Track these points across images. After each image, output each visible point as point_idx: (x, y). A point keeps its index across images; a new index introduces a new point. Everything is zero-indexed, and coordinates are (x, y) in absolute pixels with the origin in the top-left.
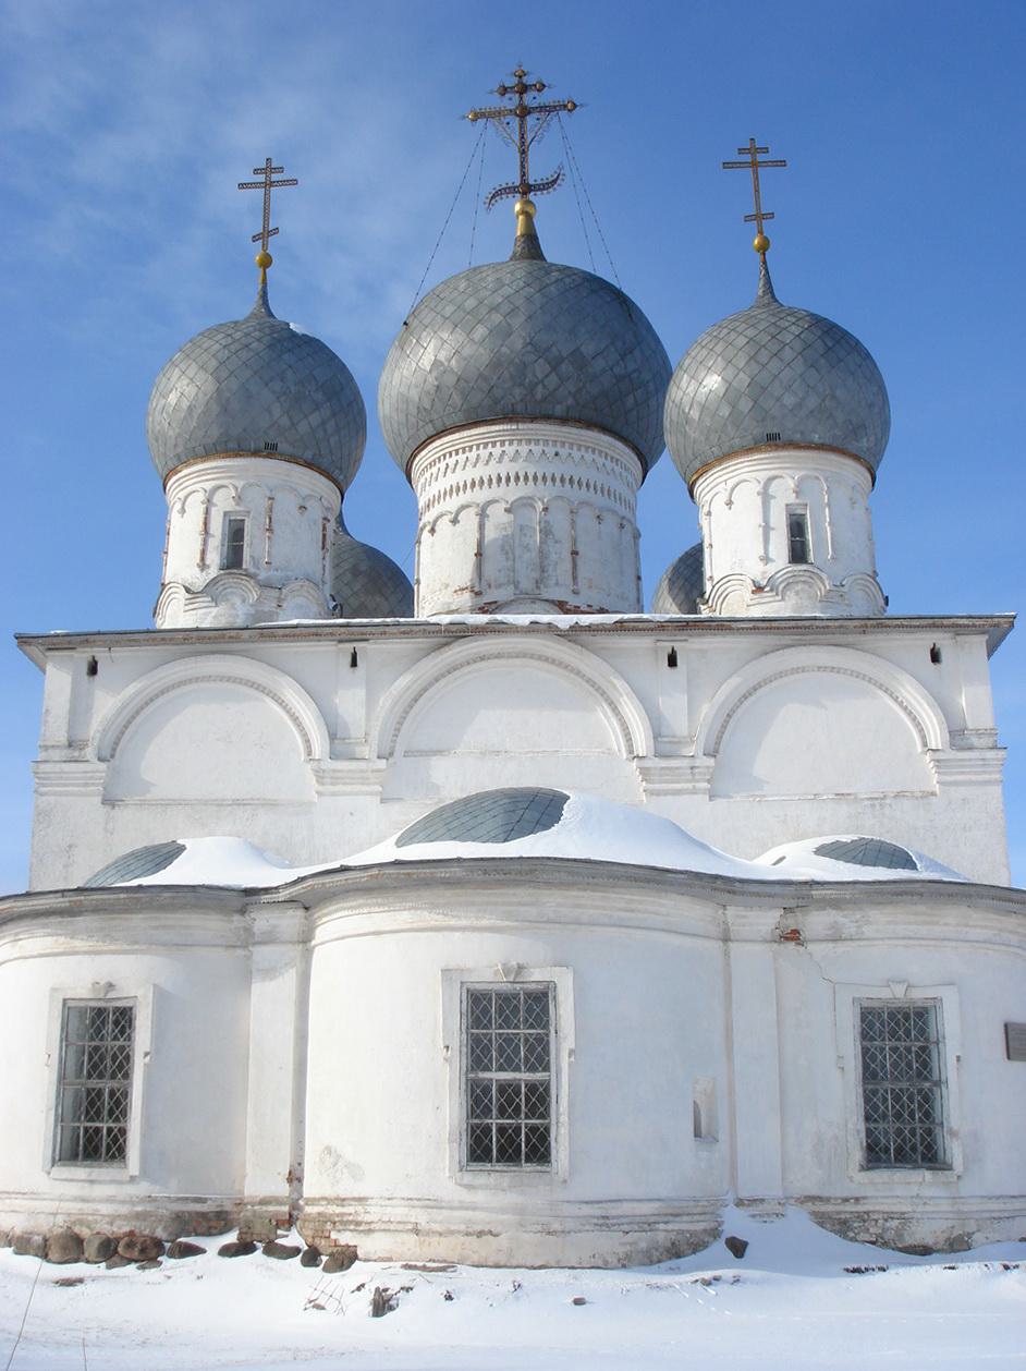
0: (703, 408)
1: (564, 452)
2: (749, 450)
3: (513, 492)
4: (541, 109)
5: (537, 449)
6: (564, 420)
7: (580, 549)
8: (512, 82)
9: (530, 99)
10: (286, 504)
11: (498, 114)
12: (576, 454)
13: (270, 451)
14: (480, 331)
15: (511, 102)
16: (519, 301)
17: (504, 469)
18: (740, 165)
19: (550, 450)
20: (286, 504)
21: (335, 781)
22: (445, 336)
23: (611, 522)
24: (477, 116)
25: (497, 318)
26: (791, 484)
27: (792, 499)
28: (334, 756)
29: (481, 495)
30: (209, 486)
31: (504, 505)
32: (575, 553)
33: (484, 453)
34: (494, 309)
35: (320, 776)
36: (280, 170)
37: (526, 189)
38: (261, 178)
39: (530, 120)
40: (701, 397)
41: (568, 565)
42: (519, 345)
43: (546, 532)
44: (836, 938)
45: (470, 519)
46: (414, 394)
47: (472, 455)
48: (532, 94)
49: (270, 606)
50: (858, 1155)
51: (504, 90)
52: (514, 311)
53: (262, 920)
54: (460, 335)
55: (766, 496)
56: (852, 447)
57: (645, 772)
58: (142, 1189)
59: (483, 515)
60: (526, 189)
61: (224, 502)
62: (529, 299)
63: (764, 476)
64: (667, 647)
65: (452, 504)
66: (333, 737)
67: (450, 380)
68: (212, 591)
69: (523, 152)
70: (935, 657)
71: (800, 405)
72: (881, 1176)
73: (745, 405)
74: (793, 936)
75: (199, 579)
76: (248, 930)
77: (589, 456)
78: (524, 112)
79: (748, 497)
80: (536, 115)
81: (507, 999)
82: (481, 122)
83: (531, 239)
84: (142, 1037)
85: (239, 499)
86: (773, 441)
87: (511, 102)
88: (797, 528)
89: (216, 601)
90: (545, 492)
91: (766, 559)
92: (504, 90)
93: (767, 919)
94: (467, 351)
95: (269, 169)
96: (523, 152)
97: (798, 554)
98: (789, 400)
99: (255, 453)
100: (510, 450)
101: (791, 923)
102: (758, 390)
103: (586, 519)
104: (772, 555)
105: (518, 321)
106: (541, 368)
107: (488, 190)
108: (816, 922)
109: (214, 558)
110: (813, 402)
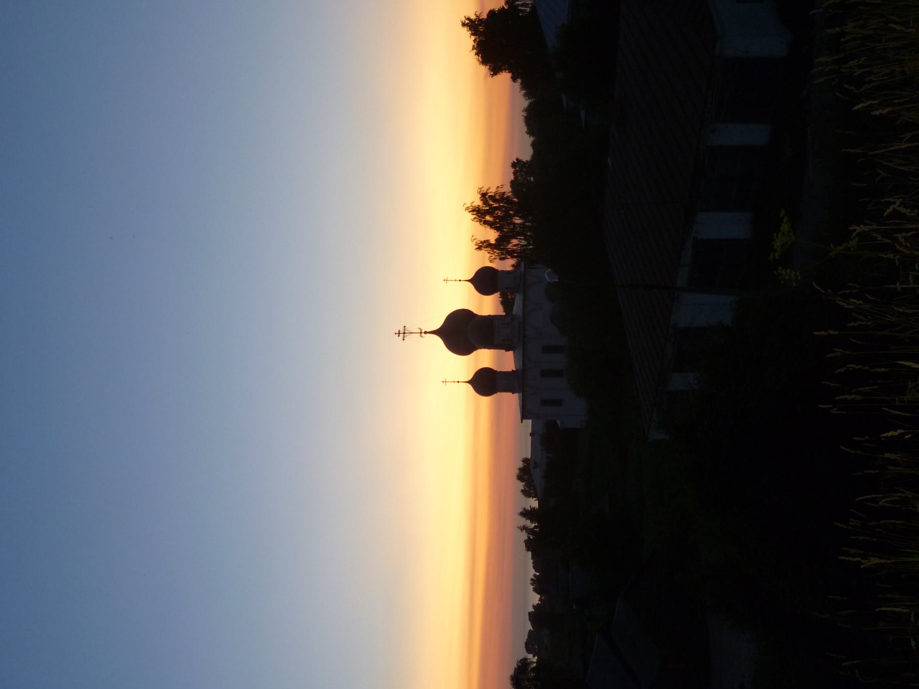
8: (397, 335)
11: (404, 337)
15: (402, 335)
24: (404, 340)
37: (421, 333)
39: (406, 332)
48: (401, 332)
69: (413, 333)
87: (402, 335)
92: (399, 336)
96: (413, 333)
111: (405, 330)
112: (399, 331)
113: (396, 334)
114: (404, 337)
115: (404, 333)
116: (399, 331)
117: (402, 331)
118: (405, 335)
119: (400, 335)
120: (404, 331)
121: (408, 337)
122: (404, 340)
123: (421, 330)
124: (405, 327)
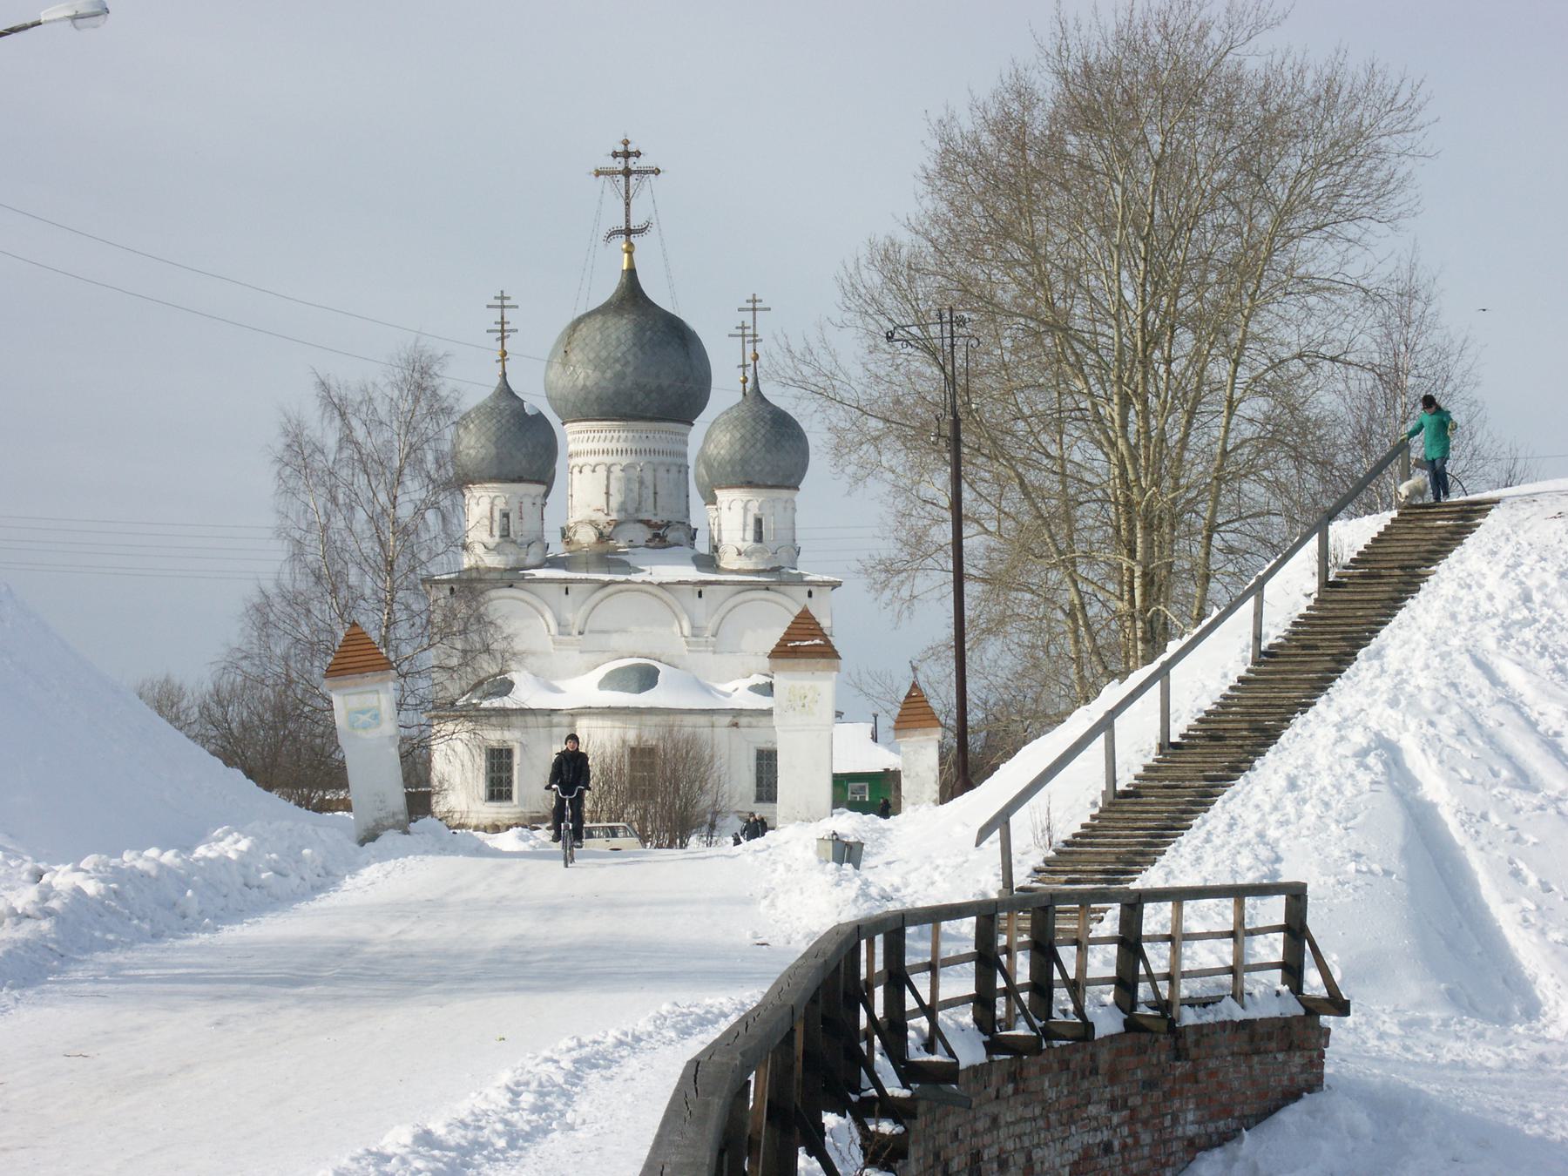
0: (720, 463)
1: (650, 436)
2: (741, 487)
3: (625, 460)
4: (639, 172)
5: (637, 435)
6: (652, 419)
7: (658, 489)
8: (620, 148)
9: (633, 163)
10: (527, 503)
11: (611, 173)
12: (657, 436)
13: (520, 480)
14: (609, 374)
15: (619, 164)
16: (630, 358)
17: (620, 446)
18: (748, 310)
19: (644, 435)
20: (527, 503)
21: (560, 643)
22: (590, 372)
23: (674, 470)
24: (598, 173)
25: (618, 367)
26: (757, 504)
27: (756, 511)
28: (561, 634)
29: (608, 459)
30: (492, 495)
31: (619, 467)
32: (655, 493)
33: (609, 435)
34: (617, 360)
35: (554, 642)
36: (508, 298)
37: (628, 232)
38: (498, 302)
39: (632, 179)
40: (720, 457)
41: (652, 500)
42: (629, 384)
43: (641, 483)
44: (749, 726)
45: (602, 471)
46: (572, 398)
47: (603, 435)
48: (632, 160)
49: (523, 556)
50: (753, 798)
51: (615, 155)
52: (627, 364)
53: (556, 719)
54: (598, 374)
55: (746, 509)
56: (787, 484)
57: (687, 642)
58: (518, 810)
59: (609, 471)
60: (628, 232)
61: (500, 504)
62: (635, 355)
63: (745, 499)
64: (698, 589)
65: (593, 460)
66: (559, 625)
67: (592, 397)
68: (497, 549)
69: (628, 204)
70: (810, 594)
71: (761, 471)
72: (760, 805)
73: (738, 468)
74: (736, 725)
75: (492, 542)
76: (551, 722)
77: (663, 436)
78: (627, 173)
79: (738, 507)
80: (635, 176)
81: (642, 750)
82: (602, 177)
83: (631, 273)
84: (516, 759)
85: (506, 503)
86: (750, 484)
87: (619, 164)
88: (759, 522)
89: (499, 554)
90: (642, 461)
91: (744, 540)
92: (615, 155)
93: (727, 720)
94: (603, 384)
95: (502, 298)
96: (628, 204)
97: (759, 537)
98: (758, 468)
99: (513, 481)
100: (623, 435)
101: (735, 720)
102: (744, 461)
103: (662, 473)
104: (747, 538)
105: (630, 370)
106: (640, 396)
107: (604, 232)
108: (743, 721)
109: (497, 532)
110: (768, 468)
111: (642, 172)
112: (638, 154)
113: (626, 143)
114: (611, 173)
115: (627, 173)
116: (638, 154)
117: (633, 163)
118: (621, 178)
119: (622, 160)
120: (635, 172)
121: (611, 192)
122: (598, 173)
123: (641, 231)
124: (657, 172)
